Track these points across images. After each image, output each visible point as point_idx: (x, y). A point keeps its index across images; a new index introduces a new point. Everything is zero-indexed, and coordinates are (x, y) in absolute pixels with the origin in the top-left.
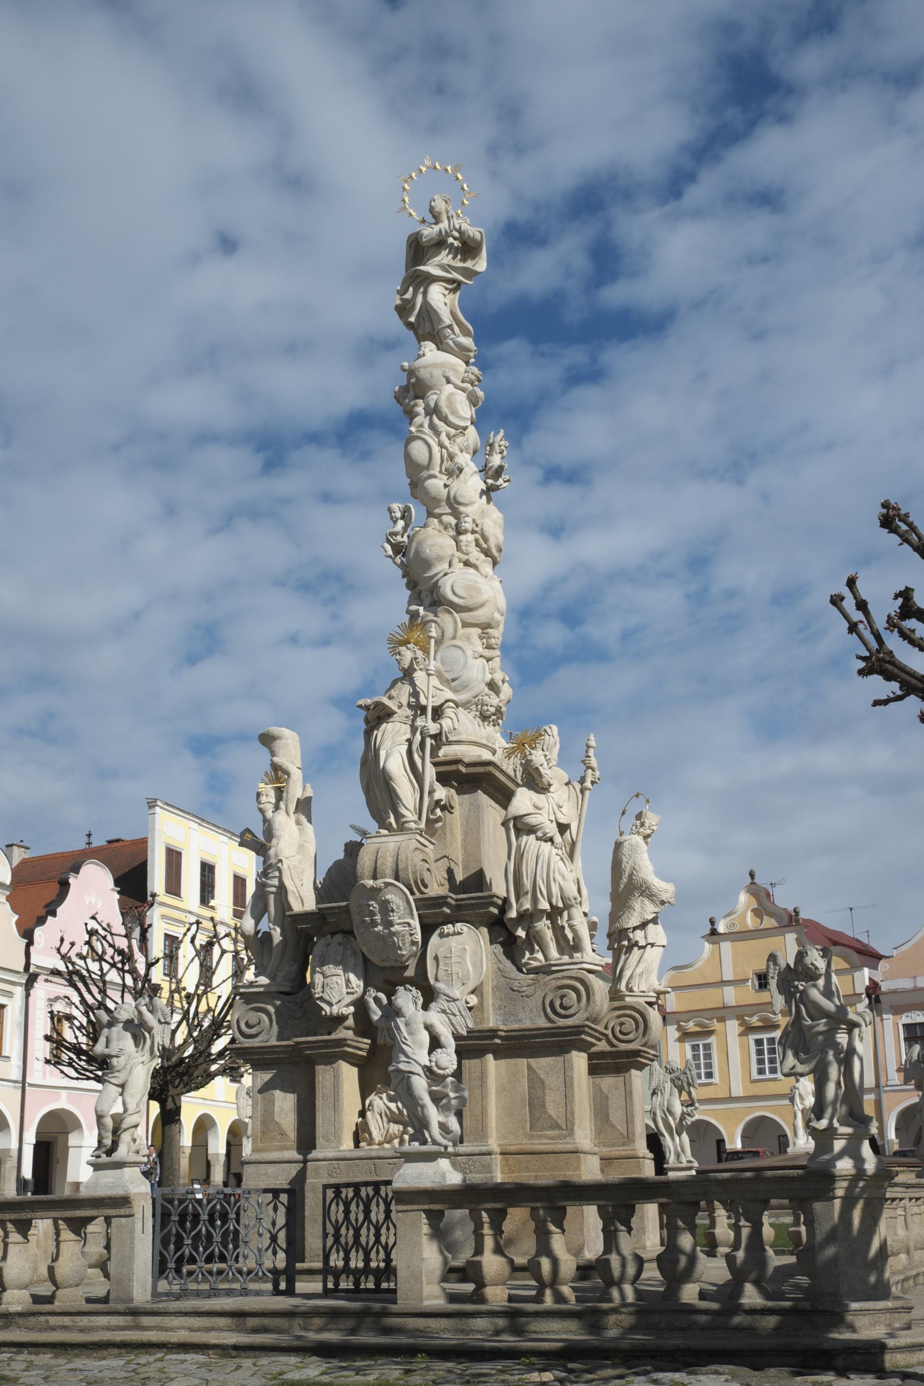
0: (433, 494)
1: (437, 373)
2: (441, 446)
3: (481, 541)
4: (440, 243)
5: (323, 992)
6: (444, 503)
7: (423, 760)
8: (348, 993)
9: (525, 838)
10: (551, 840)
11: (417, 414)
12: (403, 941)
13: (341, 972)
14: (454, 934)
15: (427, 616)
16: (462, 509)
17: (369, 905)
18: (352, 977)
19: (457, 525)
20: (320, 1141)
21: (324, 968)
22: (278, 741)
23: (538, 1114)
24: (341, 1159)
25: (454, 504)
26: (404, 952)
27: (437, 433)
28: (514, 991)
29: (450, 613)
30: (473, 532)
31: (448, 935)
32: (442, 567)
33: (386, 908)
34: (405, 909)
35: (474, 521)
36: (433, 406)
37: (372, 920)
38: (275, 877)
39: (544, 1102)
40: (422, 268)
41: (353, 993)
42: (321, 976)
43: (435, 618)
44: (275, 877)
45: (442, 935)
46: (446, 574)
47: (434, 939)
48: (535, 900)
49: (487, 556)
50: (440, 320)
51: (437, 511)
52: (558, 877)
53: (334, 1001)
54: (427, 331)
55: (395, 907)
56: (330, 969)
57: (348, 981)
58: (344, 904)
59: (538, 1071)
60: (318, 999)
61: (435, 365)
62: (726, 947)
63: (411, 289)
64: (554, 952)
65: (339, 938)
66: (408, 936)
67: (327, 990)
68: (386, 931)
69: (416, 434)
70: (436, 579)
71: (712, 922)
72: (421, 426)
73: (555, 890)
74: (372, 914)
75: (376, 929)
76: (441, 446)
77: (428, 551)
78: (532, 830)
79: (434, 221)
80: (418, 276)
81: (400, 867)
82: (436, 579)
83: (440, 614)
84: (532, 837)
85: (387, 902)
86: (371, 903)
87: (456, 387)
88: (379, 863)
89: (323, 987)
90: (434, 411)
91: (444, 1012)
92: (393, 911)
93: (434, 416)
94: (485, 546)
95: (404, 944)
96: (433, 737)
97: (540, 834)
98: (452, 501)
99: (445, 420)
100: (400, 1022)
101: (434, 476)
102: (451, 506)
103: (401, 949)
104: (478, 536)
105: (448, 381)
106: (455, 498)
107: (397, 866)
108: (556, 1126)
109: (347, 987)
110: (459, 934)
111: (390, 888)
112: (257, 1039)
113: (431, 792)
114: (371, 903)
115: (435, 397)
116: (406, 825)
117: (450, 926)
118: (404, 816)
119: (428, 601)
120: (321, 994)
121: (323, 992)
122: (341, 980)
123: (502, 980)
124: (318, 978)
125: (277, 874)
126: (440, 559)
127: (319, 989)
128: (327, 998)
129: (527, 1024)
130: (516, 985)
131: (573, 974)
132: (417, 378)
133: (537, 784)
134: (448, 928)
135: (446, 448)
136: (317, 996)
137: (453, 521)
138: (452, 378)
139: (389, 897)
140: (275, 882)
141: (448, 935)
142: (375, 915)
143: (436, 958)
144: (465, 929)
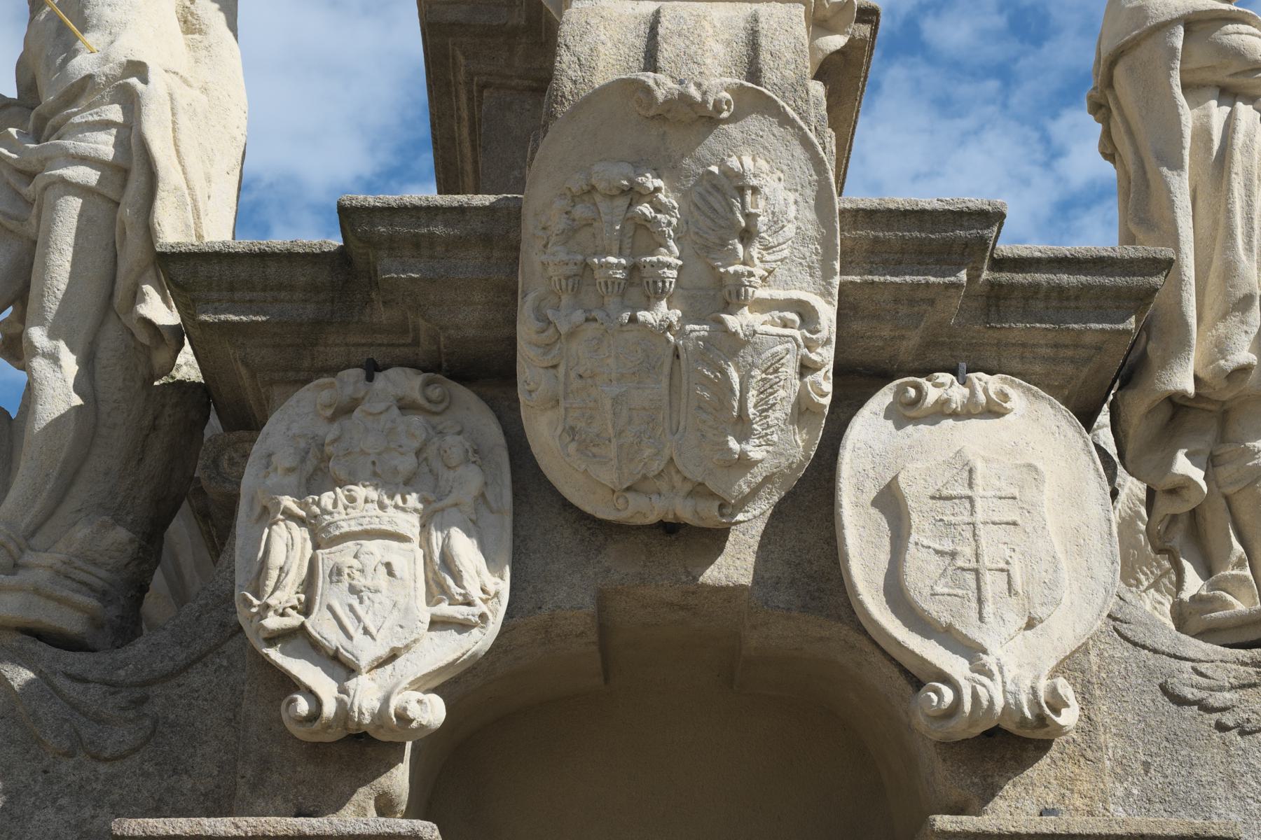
5: (306, 610)
8: (438, 624)
9: (1217, 113)
12: (767, 389)
13: (409, 524)
14: (967, 412)
17: (634, 194)
18: (465, 549)
21: (327, 499)
26: (755, 451)
28: (1180, 701)
33: (722, 213)
34: (801, 237)
37: (633, 269)
38: (106, 125)
41: (463, 626)
42: (301, 534)
44: (106, 125)
47: (869, 427)
53: (365, 651)
56: (356, 505)
57: (443, 569)
60: (275, 638)
66: (790, 369)
67: (331, 595)
68: (699, 330)
74: (644, 235)
75: (643, 315)
85: (737, 185)
86: (651, 182)
89: (309, 585)
95: (765, 408)
103: (743, 427)
109: (436, 591)
111: (755, 123)
114: (651, 182)
120: (294, 620)
122: (409, 561)
124: (287, 546)
125: (115, 113)
127: (288, 594)
134: (942, 388)
136: (273, 622)
139: (746, 162)
140: (104, 145)
141: (942, 412)
142: (658, 243)
143: (890, 502)
144: (1014, 394)
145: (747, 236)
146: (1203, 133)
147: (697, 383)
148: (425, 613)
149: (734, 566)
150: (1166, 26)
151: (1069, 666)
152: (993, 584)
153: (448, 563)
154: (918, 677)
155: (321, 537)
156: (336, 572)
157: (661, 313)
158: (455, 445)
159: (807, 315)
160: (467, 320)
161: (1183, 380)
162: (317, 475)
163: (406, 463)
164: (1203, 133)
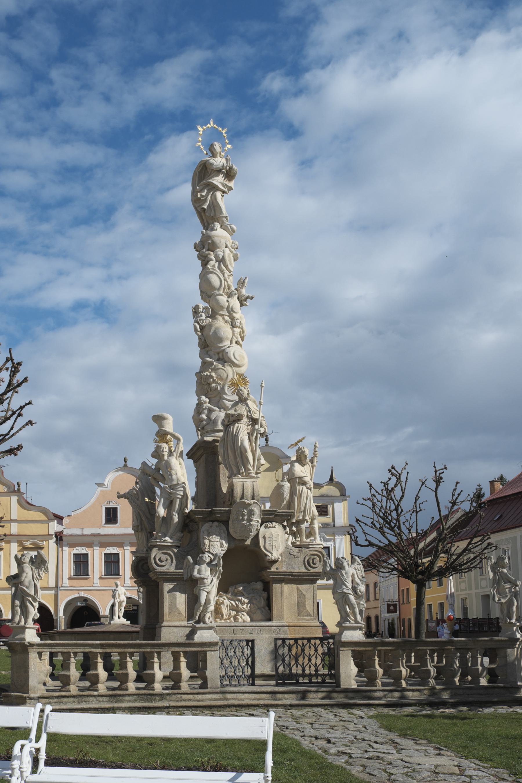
0: (222, 304)
1: (223, 241)
2: (225, 280)
5: (209, 548)
6: (225, 310)
7: (256, 444)
9: (301, 487)
11: (211, 260)
13: (218, 540)
14: (272, 527)
15: (218, 366)
16: (234, 315)
17: (244, 511)
18: (224, 542)
25: (230, 311)
26: (252, 534)
27: (223, 274)
29: (231, 366)
30: (239, 327)
31: (270, 527)
32: (227, 343)
33: (251, 513)
35: (240, 322)
40: (210, 181)
45: (266, 527)
46: (229, 347)
48: (304, 516)
50: (221, 212)
51: (221, 312)
54: (212, 215)
56: (214, 538)
57: (222, 545)
58: (227, 509)
59: (303, 591)
63: (206, 191)
64: (305, 539)
65: (216, 523)
67: (212, 548)
69: (211, 270)
72: (214, 266)
74: (244, 515)
76: (225, 280)
80: (209, 185)
81: (255, 495)
83: (226, 366)
84: (304, 487)
85: (253, 511)
86: (245, 510)
88: (245, 491)
89: (209, 546)
90: (221, 261)
96: (260, 434)
97: (308, 486)
98: (230, 309)
101: (222, 295)
102: (229, 312)
103: (251, 532)
105: (226, 247)
106: (232, 308)
107: (254, 494)
108: (310, 615)
109: (221, 547)
110: (275, 527)
111: (255, 504)
112: (164, 568)
113: (259, 460)
114: (245, 510)
116: (251, 474)
117: (270, 523)
118: (250, 470)
119: (217, 357)
121: (209, 548)
124: (207, 542)
125: (182, 489)
126: (227, 339)
127: (207, 547)
128: (212, 552)
129: (296, 570)
131: (317, 549)
132: (212, 241)
134: (270, 524)
135: (227, 282)
136: (206, 550)
139: (254, 508)
140: (181, 493)
141: (270, 527)
143: (264, 537)
145: (253, 515)
146: (299, 490)
147: (247, 529)
148: (220, 549)
149: (248, 542)
150: (297, 478)
151: (281, 555)
152: (274, 547)
153: (222, 544)
154: (266, 555)
155: (210, 541)
157: (245, 522)
158: (222, 531)
159: (258, 521)
160: (224, 519)
161: (294, 521)
162: (209, 535)
163: (218, 534)
164: (299, 490)
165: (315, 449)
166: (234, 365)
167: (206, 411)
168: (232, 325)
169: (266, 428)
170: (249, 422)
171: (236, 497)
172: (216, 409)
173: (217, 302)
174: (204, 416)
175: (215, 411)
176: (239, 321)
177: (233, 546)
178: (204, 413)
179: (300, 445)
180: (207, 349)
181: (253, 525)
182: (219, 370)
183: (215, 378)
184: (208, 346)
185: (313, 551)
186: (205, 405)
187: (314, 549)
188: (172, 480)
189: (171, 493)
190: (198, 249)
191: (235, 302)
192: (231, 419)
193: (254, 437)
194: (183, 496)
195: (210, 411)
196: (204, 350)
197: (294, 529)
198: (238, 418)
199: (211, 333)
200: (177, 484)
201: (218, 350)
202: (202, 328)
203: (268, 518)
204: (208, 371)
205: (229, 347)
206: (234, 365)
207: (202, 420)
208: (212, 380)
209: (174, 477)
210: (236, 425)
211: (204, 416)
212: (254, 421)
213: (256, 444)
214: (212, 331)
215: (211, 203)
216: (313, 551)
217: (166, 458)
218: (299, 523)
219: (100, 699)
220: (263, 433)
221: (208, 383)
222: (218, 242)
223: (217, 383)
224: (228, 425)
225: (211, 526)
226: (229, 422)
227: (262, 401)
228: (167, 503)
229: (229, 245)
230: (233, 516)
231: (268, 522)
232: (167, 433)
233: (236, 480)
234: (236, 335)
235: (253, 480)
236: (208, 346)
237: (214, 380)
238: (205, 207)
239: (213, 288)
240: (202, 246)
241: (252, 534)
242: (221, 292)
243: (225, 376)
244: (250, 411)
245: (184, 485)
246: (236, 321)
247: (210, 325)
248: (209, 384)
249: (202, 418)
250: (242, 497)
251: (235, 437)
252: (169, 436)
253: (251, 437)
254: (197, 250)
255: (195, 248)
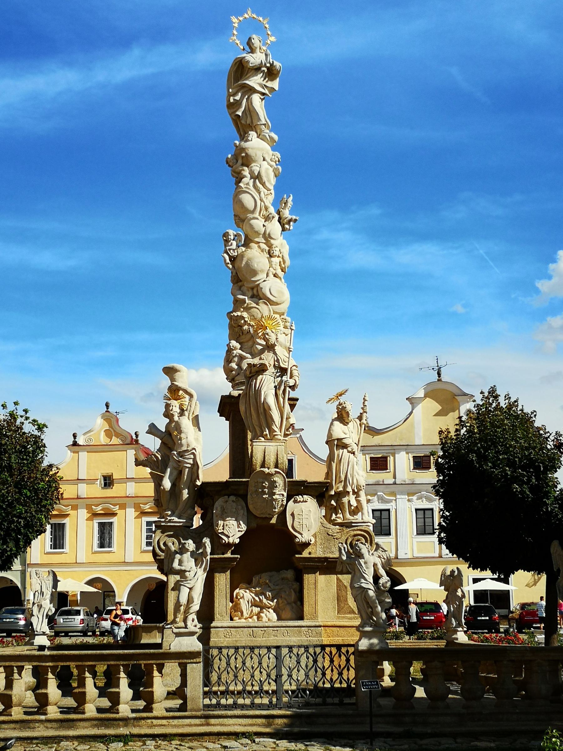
0: (256, 230)
2: (261, 200)
3: (282, 263)
4: (257, 69)
5: (223, 529)
6: (261, 236)
7: (284, 399)
8: (239, 531)
9: (341, 451)
10: (354, 453)
11: (245, 177)
12: (278, 504)
14: (303, 501)
16: (272, 241)
19: (269, 251)
20: (217, 616)
22: (178, 373)
23: (343, 605)
24: (232, 627)
25: (268, 237)
26: (276, 510)
27: (260, 193)
28: (329, 535)
29: (267, 305)
30: (279, 257)
31: (300, 501)
32: (261, 276)
33: (273, 485)
36: (256, 174)
39: (347, 599)
41: (242, 531)
43: (257, 306)
45: (296, 502)
46: (264, 281)
47: (291, 503)
48: (345, 486)
49: (282, 271)
50: (259, 119)
51: (257, 240)
52: (356, 475)
53: (231, 535)
54: (248, 123)
55: (278, 485)
59: (343, 581)
60: (220, 533)
61: (259, 149)
62: (83, 455)
63: (240, 94)
64: (348, 516)
65: (232, 498)
66: (280, 501)
69: (244, 189)
70: (258, 283)
71: (75, 436)
72: (248, 184)
73: (355, 481)
76: (261, 200)
77: (256, 266)
78: (345, 446)
79: (249, 51)
81: (279, 462)
82: (258, 283)
83: (260, 304)
84: (345, 450)
85: (275, 482)
87: (268, 164)
88: (266, 458)
89: (223, 526)
90: (257, 177)
91: (379, 557)
92: (276, 487)
93: (257, 180)
94: (283, 266)
95: (277, 506)
96: (290, 387)
97: (349, 449)
98: (267, 236)
99: (263, 184)
100: (362, 561)
101: (257, 219)
102: (265, 239)
103: (275, 508)
104: (282, 260)
105: (264, 160)
106: (269, 234)
107: (277, 461)
110: (306, 502)
111: (278, 475)
115: (258, 169)
116: (276, 437)
117: (300, 496)
119: (250, 294)
120: (222, 531)
121: (223, 529)
123: (323, 528)
125: (192, 456)
126: (262, 271)
127: (221, 528)
128: (227, 533)
130: (330, 532)
131: (363, 528)
132: (246, 154)
133: (344, 420)
134: (299, 498)
136: (219, 531)
137: (267, 249)
138: (267, 158)
140: (191, 461)
141: (300, 501)
144: (309, 499)
145: (276, 487)
146: (338, 455)
148: (237, 530)
149: (274, 521)
150: (334, 440)
153: (240, 524)
154: (296, 537)
156: (227, 525)
158: (240, 507)
159: (283, 495)
160: (241, 492)
161: (333, 493)
164: (338, 455)
165: (364, 403)
166: (269, 302)
167: (236, 359)
168: (269, 253)
169: (297, 379)
170: (277, 373)
171: (256, 465)
172: (248, 356)
173: (251, 226)
174: (234, 365)
175: (247, 358)
176: (277, 249)
177: (254, 525)
178: (234, 361)
179: (342, 399)
180: (240, 284)
181: (276, 499)
182: (252, 310)
183: (246, 319)
184: (241, 281)
185: (358, 530)
186: (235, 352)
187: (358, 528)
188: (181, 445)
189: (179, 461)
190: (231, 164)
191: (275, 227)
192: (254, 369)
193: (281, 391)
194: (193, 465)
195: (242, 358)
196: (236, 285)
197: (333, 502)
198: (262, 369)
199: (243, 265)
200: (187, 451)
201: (252, 285)
202: (233, 259)
203: (297, 489)
204: (239, 310)
205: (264, 281)
206: (269, 302)
207: (232, 370)
208: (243, 321)
209: (184, 441)
210: (260, 377)
211: (234, 365)
212: (283, 371)
213: (284, 399)
214: (244, 263)
215: (247, 109)
216: (358, 530)
217: (176, 418)
218: (339, 495)
219: (49, 725)
220: (293, 386)
221: (239, 326)
222: (254, 155)
223: (249, 325)
224: (250, 377)
225: (227, 501)
226: (250, 373)
227: (291, 347)
228: (175, 473)
229: (268, 159)
230: (251, 488)
231: (298, 495)
232: (178, 389)
233: (257, 443)
234: (274, 266)
235: (278, 444)
236: (241, 281)
237: (245, 321)
238: (240, 113)
239: (247, 211)
240: (235, 161)
241: (276, 510)
242: (257, 215)
243: (260, 316)
244: (278, 361)
245: (194, 451)
246: (273, 249)
247: (242, 256)
248: (241, 326)
249: (231, 367)
250: (263, 465)
251: (258, 392)
252: (181, 392)
253: (278, 391)
254: (229, 166)
255: (227, 163)
